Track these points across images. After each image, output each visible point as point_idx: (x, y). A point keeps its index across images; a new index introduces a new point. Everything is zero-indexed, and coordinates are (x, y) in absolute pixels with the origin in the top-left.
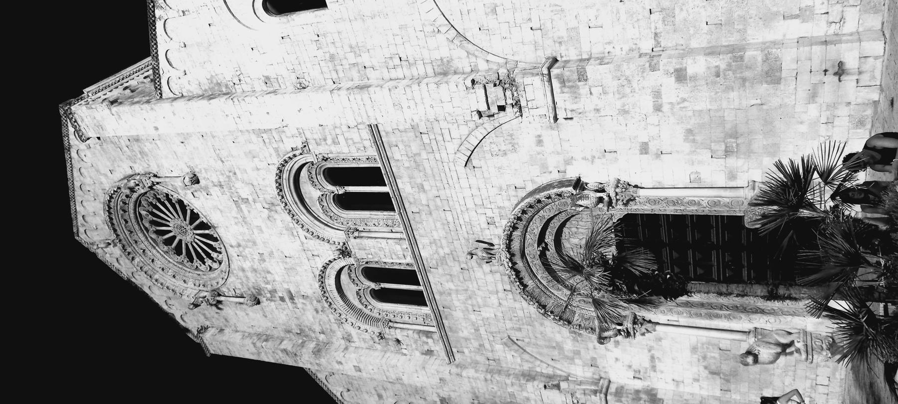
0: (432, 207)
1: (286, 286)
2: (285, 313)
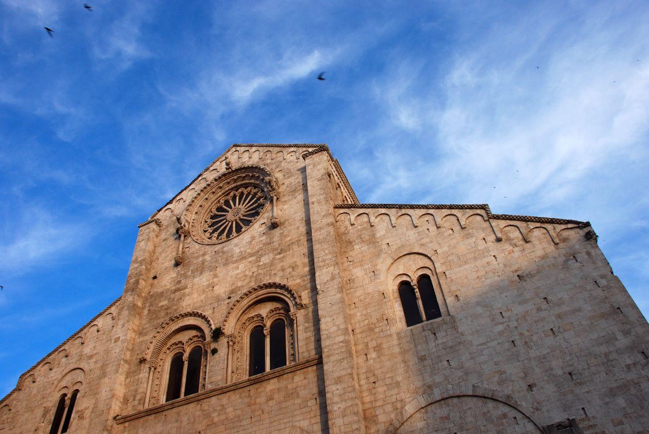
0: (253, 407)
1: (189, 286)
2: (168, 284)
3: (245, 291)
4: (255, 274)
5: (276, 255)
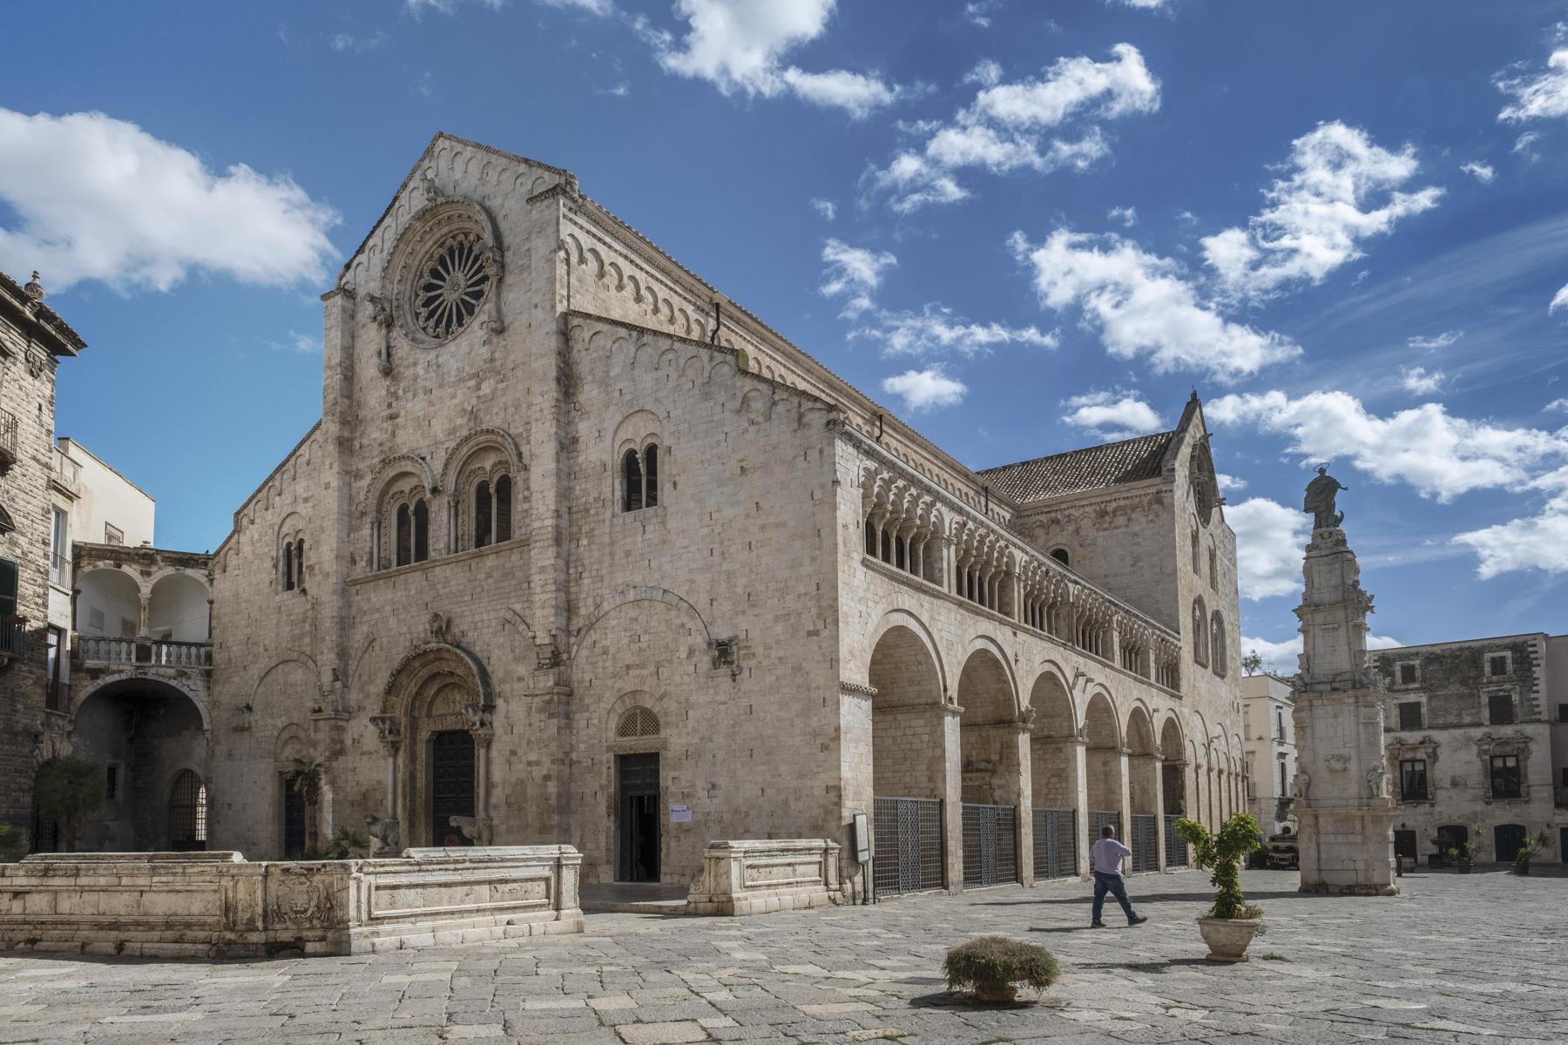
3: (465, 433)
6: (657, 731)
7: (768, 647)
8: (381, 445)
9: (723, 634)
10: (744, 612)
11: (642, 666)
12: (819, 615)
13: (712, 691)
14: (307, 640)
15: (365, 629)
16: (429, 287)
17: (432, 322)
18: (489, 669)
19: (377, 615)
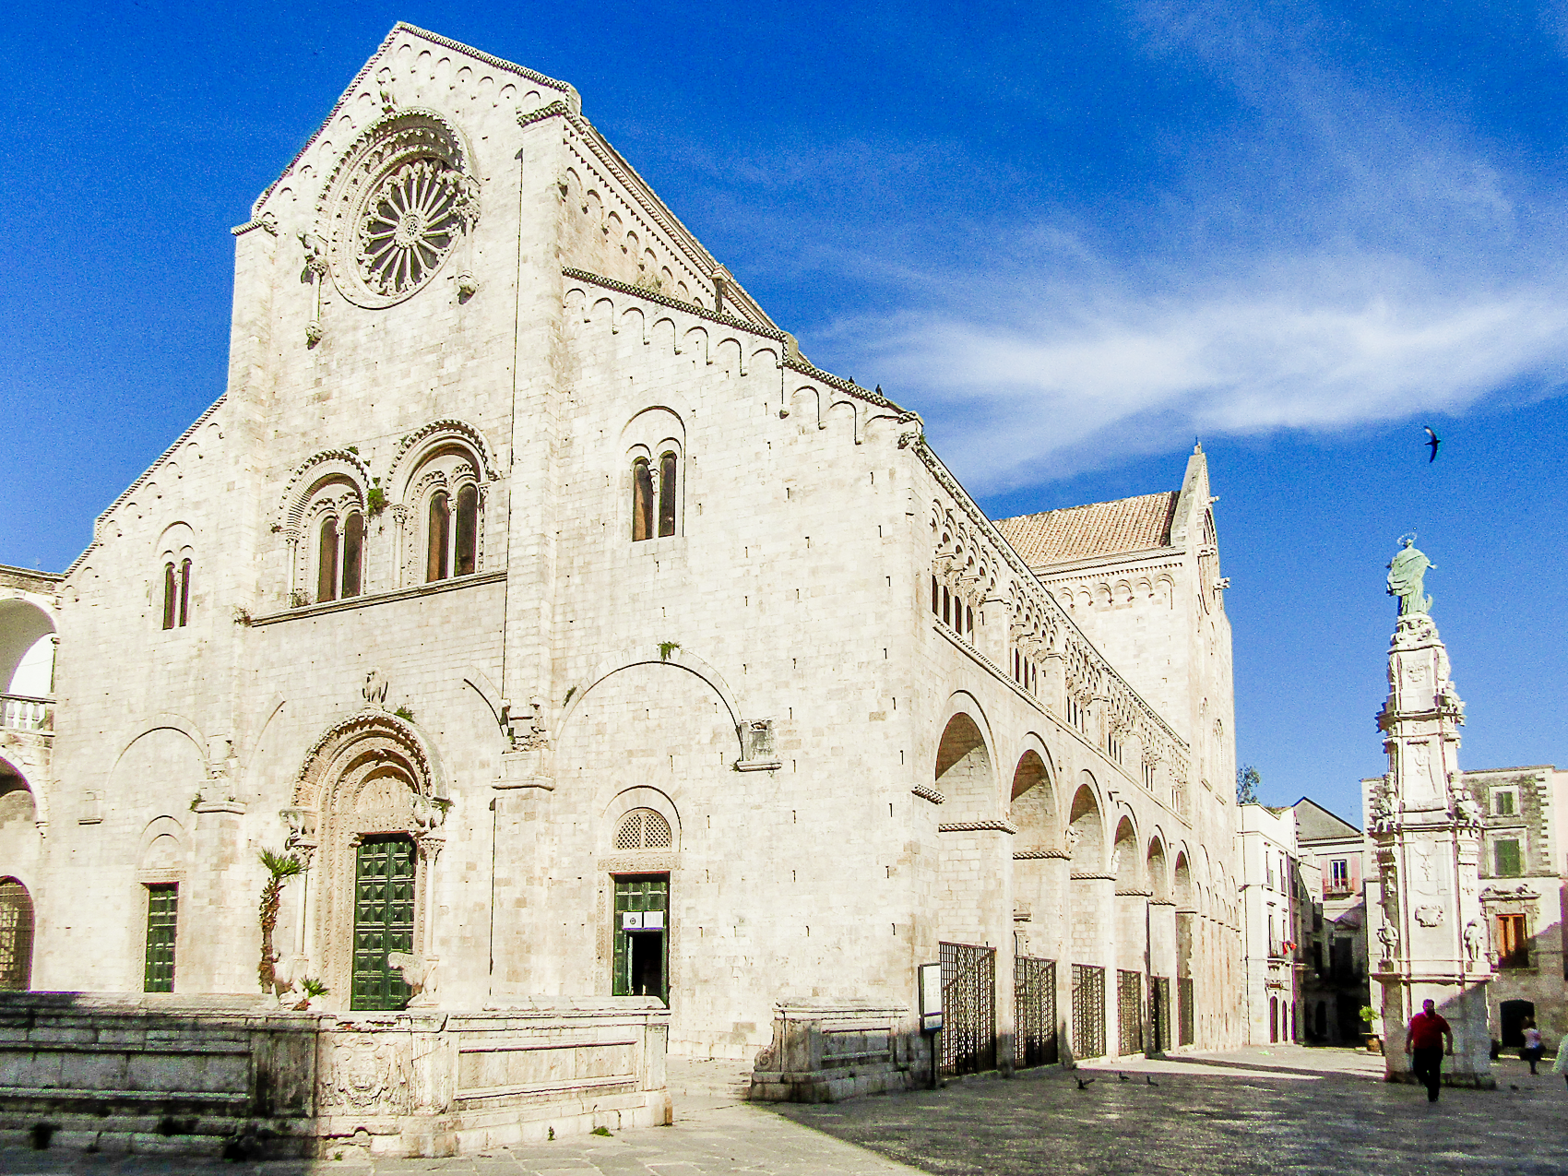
1: (335, 394)
3: (421, 425)
4: (434, 394)
5: (467, 359)
6: (667, 841)
7: (818, 732)
8: (304, 434)
9: (753, 712)
10: (787, 685)
11: (647, 752)
12: (885, 692)
13: (742, 790)
14: (190, 700)
15: (272, 686)
16: (375, 226)
17: (377, 275)
18: (442, 749)
19: (289, 669)
